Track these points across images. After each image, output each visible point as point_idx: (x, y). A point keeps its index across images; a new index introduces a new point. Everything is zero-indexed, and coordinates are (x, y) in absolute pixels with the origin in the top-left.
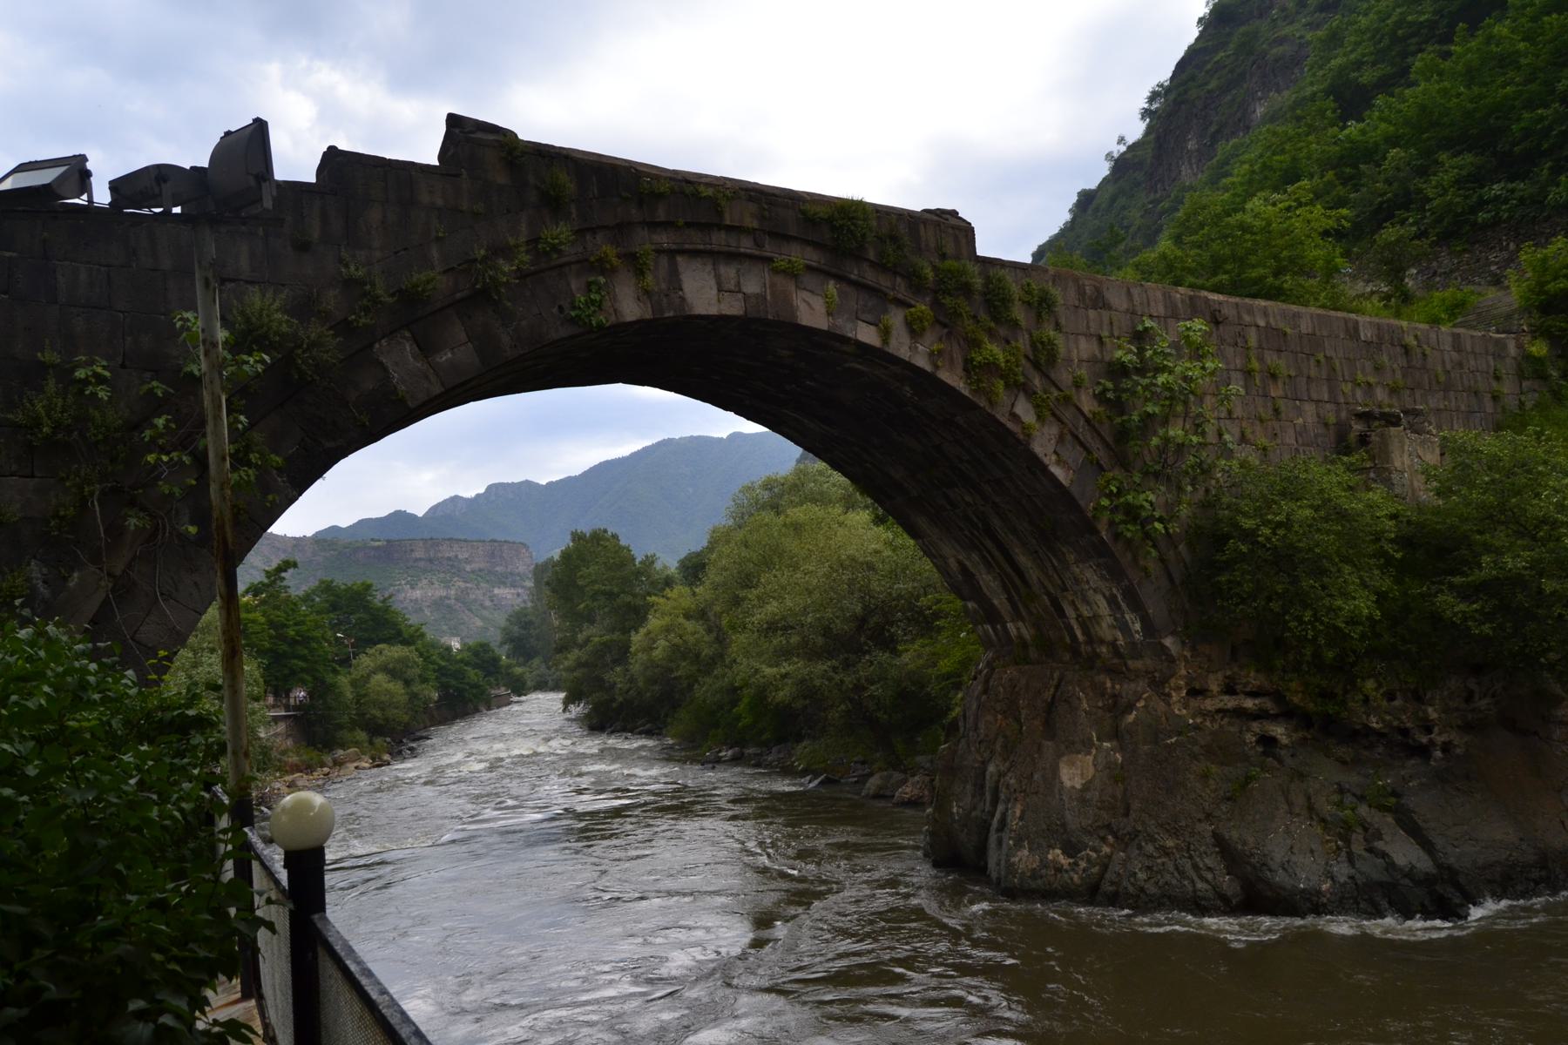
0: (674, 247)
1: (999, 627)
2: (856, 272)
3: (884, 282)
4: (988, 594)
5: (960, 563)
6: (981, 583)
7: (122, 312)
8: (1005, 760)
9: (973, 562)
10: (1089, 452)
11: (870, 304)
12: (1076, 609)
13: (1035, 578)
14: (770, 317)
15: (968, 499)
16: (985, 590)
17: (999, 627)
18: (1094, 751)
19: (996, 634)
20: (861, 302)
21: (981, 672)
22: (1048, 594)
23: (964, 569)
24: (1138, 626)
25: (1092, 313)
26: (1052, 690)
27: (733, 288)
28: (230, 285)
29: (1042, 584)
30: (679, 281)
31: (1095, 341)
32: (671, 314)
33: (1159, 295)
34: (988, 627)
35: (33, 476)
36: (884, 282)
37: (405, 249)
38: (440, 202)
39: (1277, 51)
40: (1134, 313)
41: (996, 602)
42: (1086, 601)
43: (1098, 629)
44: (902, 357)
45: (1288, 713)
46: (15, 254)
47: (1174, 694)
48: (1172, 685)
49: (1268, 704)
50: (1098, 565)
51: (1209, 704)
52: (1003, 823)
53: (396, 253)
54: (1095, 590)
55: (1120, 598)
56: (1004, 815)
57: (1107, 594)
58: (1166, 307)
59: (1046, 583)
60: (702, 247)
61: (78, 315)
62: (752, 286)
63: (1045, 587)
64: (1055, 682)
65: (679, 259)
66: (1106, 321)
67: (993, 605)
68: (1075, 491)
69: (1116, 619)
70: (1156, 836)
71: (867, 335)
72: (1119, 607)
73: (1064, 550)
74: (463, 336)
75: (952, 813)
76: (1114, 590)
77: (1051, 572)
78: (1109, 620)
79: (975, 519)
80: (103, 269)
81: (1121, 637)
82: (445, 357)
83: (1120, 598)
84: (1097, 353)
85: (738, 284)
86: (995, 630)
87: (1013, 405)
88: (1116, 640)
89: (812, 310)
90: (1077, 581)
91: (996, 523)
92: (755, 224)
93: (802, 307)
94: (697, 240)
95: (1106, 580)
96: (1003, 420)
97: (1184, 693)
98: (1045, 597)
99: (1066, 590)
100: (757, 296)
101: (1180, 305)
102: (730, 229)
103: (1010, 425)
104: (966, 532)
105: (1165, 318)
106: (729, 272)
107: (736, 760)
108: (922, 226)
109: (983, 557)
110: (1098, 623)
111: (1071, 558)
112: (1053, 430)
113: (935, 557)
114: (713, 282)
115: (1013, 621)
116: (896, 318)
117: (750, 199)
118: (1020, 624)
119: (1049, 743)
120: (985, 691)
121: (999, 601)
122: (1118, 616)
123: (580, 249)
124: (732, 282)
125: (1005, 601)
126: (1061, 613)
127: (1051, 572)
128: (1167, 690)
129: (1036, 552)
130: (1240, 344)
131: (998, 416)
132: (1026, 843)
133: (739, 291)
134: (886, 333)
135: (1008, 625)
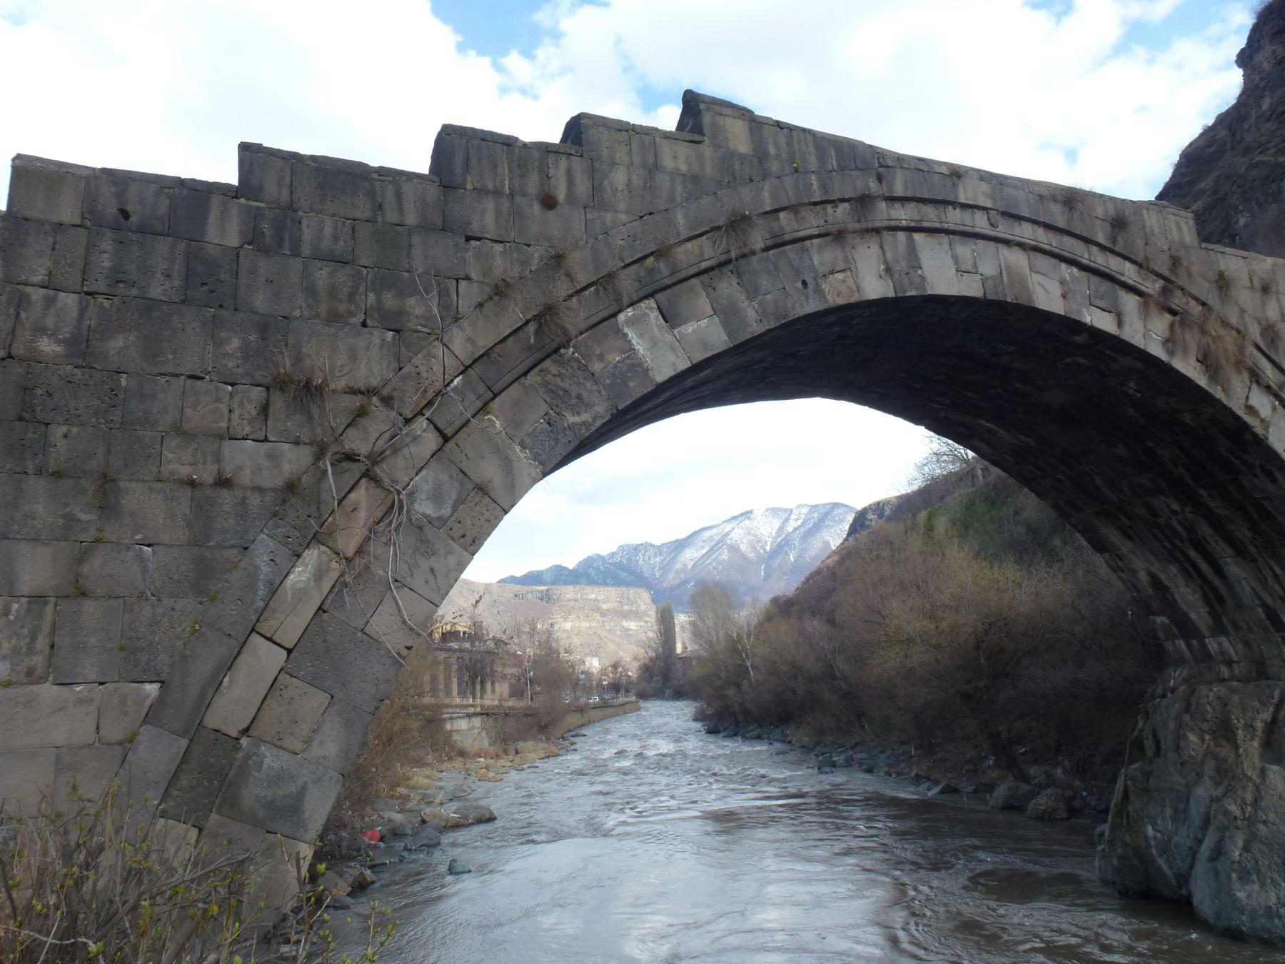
0: (913, 224)
2: (1087, 256)
3: (1113, 264)
4: (1185, 608)
5: (1153, 576)
7: (365, 267)
8: (1217, 784)
9: (1171, 575)
13: (1248, 589)
14: (1009, 300)
15: (1176, 506)
19: (1191, 650)
21: (1173, 690)
22: (1264, 605)
26: (1272, 709)
27: (970, 269)
28: (474, 243)
29: (1257, 594)
30: (918, 259)
32: (913, 293)
34: (1181, 643)
35: (266, 440)
36: (1113, 264)
37: (651, 214)
38: (684, 168)
39: (1254, 173)
41: (1193, 616)
44: (1137, 345)
46: (262, 205)
52: (1218, 853)
53: (641, 217)
56: (1221, 841)
59: (1262, 594)
60: (937, 225)
61: (321, 269)
62: (988, 269)
63: (1260, 598)
64: (1275, 701)
71: (1103, 322)
74: (709, 310)
75: (1146, 837)
77: (1270, 580)
79: (1180, 529)
80: (348, 221)
82: (690, 328)
85: (975, 265)
86: (1188, 645)
87: (1247, 398)
94: (931, 215)
96: (1241, 413)
98: (1260, 610)
100: (993, 277)
102: (965, 206)
103: (1248, 419)
104: (1166, 544)
106: (965, 250)
107: (849, 763)
108: (1145, 212)
109: (1184, 570)
113: (1123, 571)
114: (950, 262)
117: (981, 179)
118: (1223, 640)
119: (1275, 768)
120: (1187, 709)
121: (1198, 613)
123: (821, 222)
124: (969, 262)
125: (1206, 615)
127: (1270, 580)
131: (1235, 409)
132: (1255, 877)
133: (977, 273)
135: (1207, 640)
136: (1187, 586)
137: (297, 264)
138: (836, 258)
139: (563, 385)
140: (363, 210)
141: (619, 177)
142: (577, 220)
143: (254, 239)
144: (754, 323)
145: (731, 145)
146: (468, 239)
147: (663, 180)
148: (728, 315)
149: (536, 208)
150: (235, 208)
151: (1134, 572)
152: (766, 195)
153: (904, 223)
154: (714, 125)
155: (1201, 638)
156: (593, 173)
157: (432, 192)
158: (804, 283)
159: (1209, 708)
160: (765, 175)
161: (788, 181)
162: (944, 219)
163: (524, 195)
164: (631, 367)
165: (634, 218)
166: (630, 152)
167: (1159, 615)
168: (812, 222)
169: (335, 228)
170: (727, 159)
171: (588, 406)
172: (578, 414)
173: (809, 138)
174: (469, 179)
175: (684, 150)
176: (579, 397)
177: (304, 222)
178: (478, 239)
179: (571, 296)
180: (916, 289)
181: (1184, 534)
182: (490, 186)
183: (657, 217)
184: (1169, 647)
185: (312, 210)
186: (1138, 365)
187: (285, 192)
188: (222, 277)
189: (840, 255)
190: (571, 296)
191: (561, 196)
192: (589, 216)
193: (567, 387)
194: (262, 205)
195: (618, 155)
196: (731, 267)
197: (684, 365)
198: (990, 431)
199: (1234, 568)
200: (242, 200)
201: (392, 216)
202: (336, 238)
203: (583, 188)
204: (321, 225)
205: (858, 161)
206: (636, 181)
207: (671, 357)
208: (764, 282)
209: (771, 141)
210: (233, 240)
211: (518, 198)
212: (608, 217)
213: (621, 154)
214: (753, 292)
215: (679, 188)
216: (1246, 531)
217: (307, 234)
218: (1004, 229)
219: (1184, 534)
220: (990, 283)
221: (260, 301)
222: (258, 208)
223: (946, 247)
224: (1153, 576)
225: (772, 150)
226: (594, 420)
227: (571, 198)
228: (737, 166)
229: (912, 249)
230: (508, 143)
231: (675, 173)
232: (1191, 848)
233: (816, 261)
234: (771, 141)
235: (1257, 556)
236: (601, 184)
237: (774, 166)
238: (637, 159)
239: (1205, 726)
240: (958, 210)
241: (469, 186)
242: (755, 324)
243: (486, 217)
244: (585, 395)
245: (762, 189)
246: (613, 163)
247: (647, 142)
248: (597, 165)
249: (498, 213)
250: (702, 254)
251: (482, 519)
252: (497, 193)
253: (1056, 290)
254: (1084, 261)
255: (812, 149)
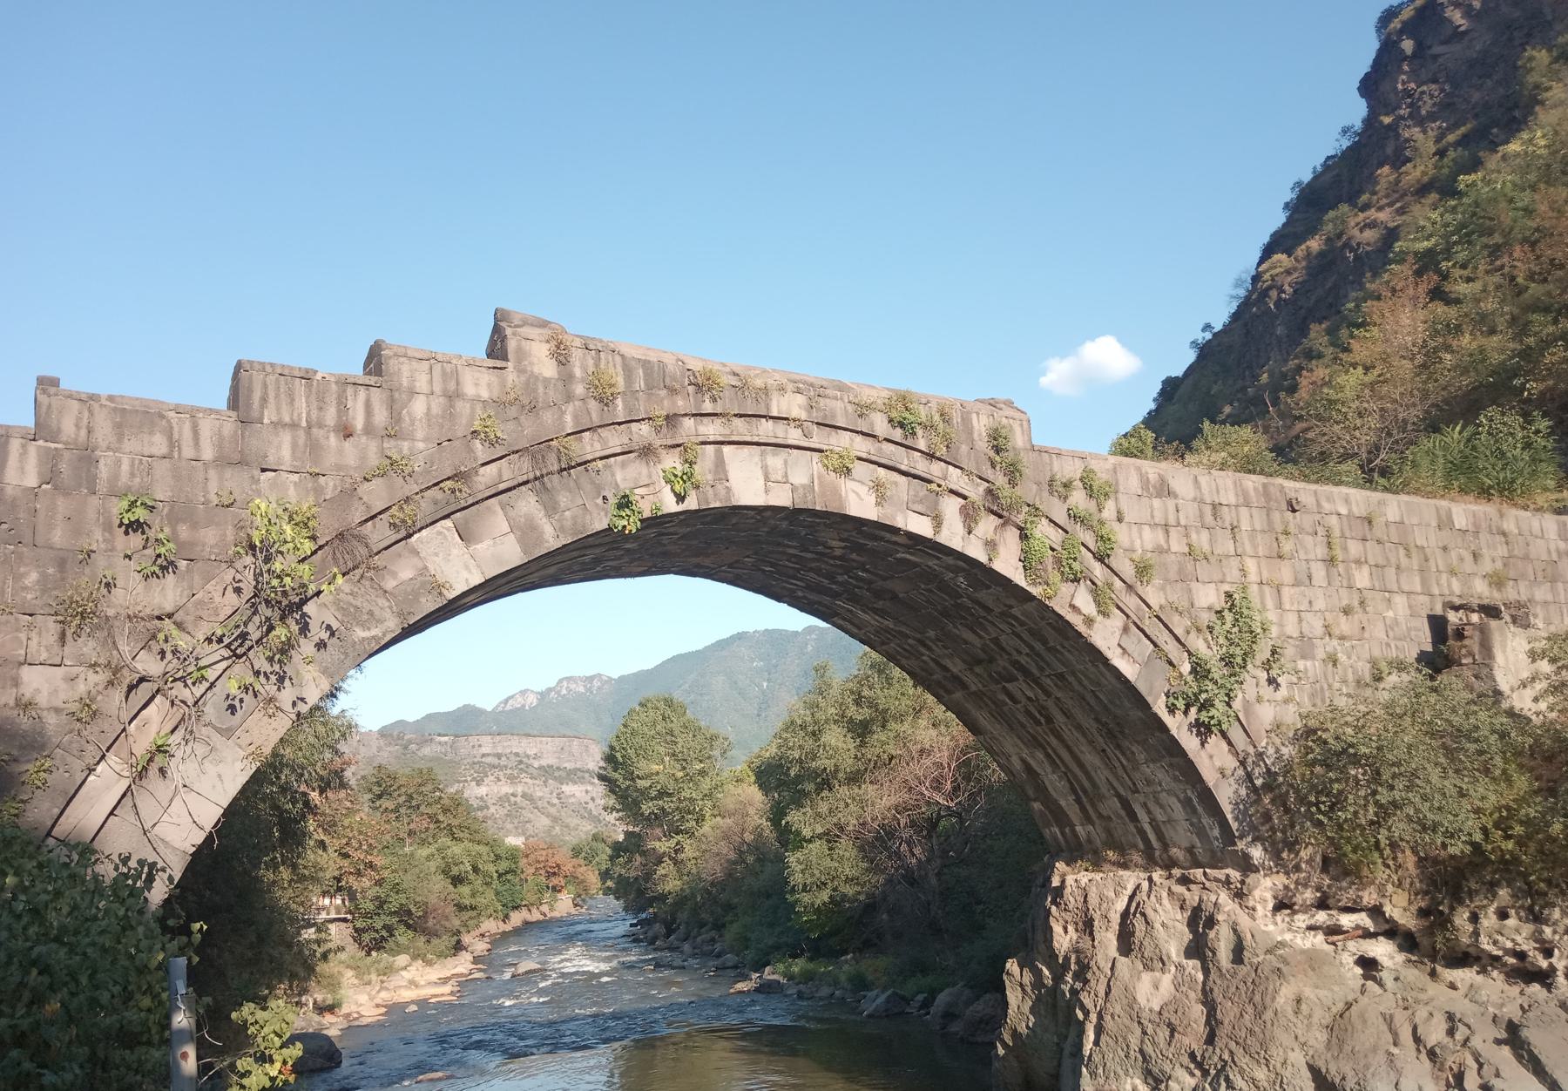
1: (1067, 830)
5: (1023, 761)
6: (1047, 783)
9: (1038, 761)
10: (1155, 645)
11: (921, 494)
12: (1149, 812)
14: (818, 508)
16: (1050, 789)
17: (1067, 830)
18: (1173, 969)
20: (911, 493)
22: (1119, 796)
23: (1028, 769)
24: (1216, 832)
25: (1156, 502)
27: (780, 479)
29: (1111, 784)
30: (725, 472)
31: (1160, 533)
32: (717, 505)
33: (1229, 483)
34: (1056, 830)
38: (485, 395)
40: (1202, 501)
41: (1063, 803)
42: (1157, 802)
43: (1172, 833)
45: (1391, 931)
46: (59, 446)
47: (1259, 907)
48: (1257, 898)
49: (1363, 919)
50: (1171, 765)
51: (1302, 920)
54: (1169, 792)
55: (1195, 801)
57: (1182, 796)
58: (1237, 495)
59: (1116, 784)
60: (748, 439)
62: (799, 478)
63: (1114, 788)
64: (1129, 892)
65: (726, 449)
66: (1172, 509)
67: (1060, 807)
68: (1142, 688)
69: (1192, 825)
70: (1245, 1067)
71: (920, 526)
72: (1194, 811)
73: (1134, 749)
76: (1189, 793)
77: (1120, 771)
78: (1186, 825)
81: (1199, 845)
82: (481, 548)
83: (1195, 801)
84: (1162, 542)
85: (786, 475)
86: (1063, 833)
87: (1073, 596)
88: (1193, 847)
89: (859, 502)
90: (1149, 783)
91: (1060, 718)
92: (804, 416)
93: (852, 497)
94: (741, 428)
95: (1180, 781)
97: (1270, 905)
99: (1137, 791)
100: (803, 486)
101: (1252, 493)
105: (1237, 506)
106: (776, 461)
108: (974, 416)
109: (1048, 756)
110: (1174, 828)
111: (1141, 757)
112: (1117, 620)
115: (1082, 825)
116: (951, 507)
117: (799, 391)
121: (1067, 803)
122: (1195, 820)
123: (627, 441)
126: (1133, 816)
128: (1251, 904)
129: (1104, 751)
130: (1320, 534)
131: (1057, 609)
134: (938, 522)
136: (1054, 772)
137: (94, 501)
138: (640, 474)
139: (354, 602)
140: (159, 445)
141: (419, 407)
142: (373, 447)
143: (51, 476)
144: (552, 539)
145: (536, 370)
146: (263, 470)
147: (462, 407)
148: (525, 532)
149: (333, 440)
150: (32, 448)
151: (1008, 757)
152: (568, 418)
153: (712, 439)
154: (519, 350)
155: (1072, 827)
156: (391, 404)
157: (229, 427)
158: (604, 498)
159: (1071, 899)
160: (569, 398)
161: (593, 405)
162: (755, 432)
163: (321, 426)
164: (423, 584)
165: (430, 446)
166: (431, 381)
167: (1035, 800)
168: (615, 440)
169: (132, 465)
170: (531, 381)
171: (380, 621)
172: (369, 629)
173: (618, 359)
174: (266, 413)
175: (486, 377)
176: (371, 613)
177: (102, 462)
178: (275, 471)
179: (366, 521)
180: (721, 501)
181: (1043, 721)
182: (287, 419)
183: (456, 443)
184: (1046, 832)
185: (109, 448)
186: (961, 563)
187: (83, 432)
188: (21, 515)
189: (644, 471)
190: (366, 521)
191: (359, 423)
192: (386, 445)
193: (359, 604)
194: (59, 446)
195: (418, 384)
196: (529, 485)
197: (477, 579)
198: (851, 611)
199: (1090, 758)
200: (41, 443)
201: (188, 452)
202: (132, 475)
203: (381, 417)
204: (118, 462)
205: (668, 380)
206: (435, 410)
207: (465, 574)
208: (563, 499)
209: (578, 364)
210: (31, 481)
211: (314, 430)
212: (405, 445)
213: (422, 383)
214: (551, 509)
215: (479, 411)
216: (1092, 722)
217: (103, 471)
218: (818, 438)
219: (1043, 721)
220: (801, 491)
221: (58, 537)
222: (56, 449)
223: (757, 459)
224: (1023, 761)
225: (578, 372)
226: (384, 635)
227: (369, 430)
228: (541, 390)
229: (720, 463)
230: (307, 376)
231: (477, 400)
232: (1058, 1044)
233: (619, 477)
234: (578, 364)
235: (1105, 747)
236: (400, 413)
237: (579, 390)
238: (437, 388)
239: (1068, 917)
240: (771, 422)
241: (266, 421)
242: (551, 540)
243: (282, 449)
244: (377, 612)
245: (563, 413)
246: (412, 393)
247: (449, 370)
248: (397, 395)
249: (294, 446)
250: (500, 475)
251: (270, 728)
252: (294, 426)
253: (871, 499)
254: (903, 468)
255: (619, 369)
